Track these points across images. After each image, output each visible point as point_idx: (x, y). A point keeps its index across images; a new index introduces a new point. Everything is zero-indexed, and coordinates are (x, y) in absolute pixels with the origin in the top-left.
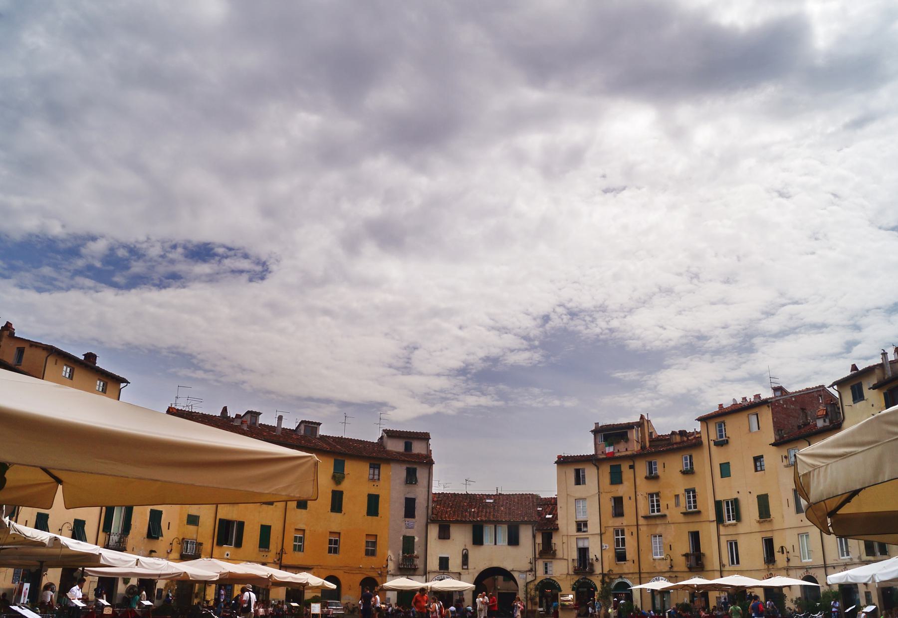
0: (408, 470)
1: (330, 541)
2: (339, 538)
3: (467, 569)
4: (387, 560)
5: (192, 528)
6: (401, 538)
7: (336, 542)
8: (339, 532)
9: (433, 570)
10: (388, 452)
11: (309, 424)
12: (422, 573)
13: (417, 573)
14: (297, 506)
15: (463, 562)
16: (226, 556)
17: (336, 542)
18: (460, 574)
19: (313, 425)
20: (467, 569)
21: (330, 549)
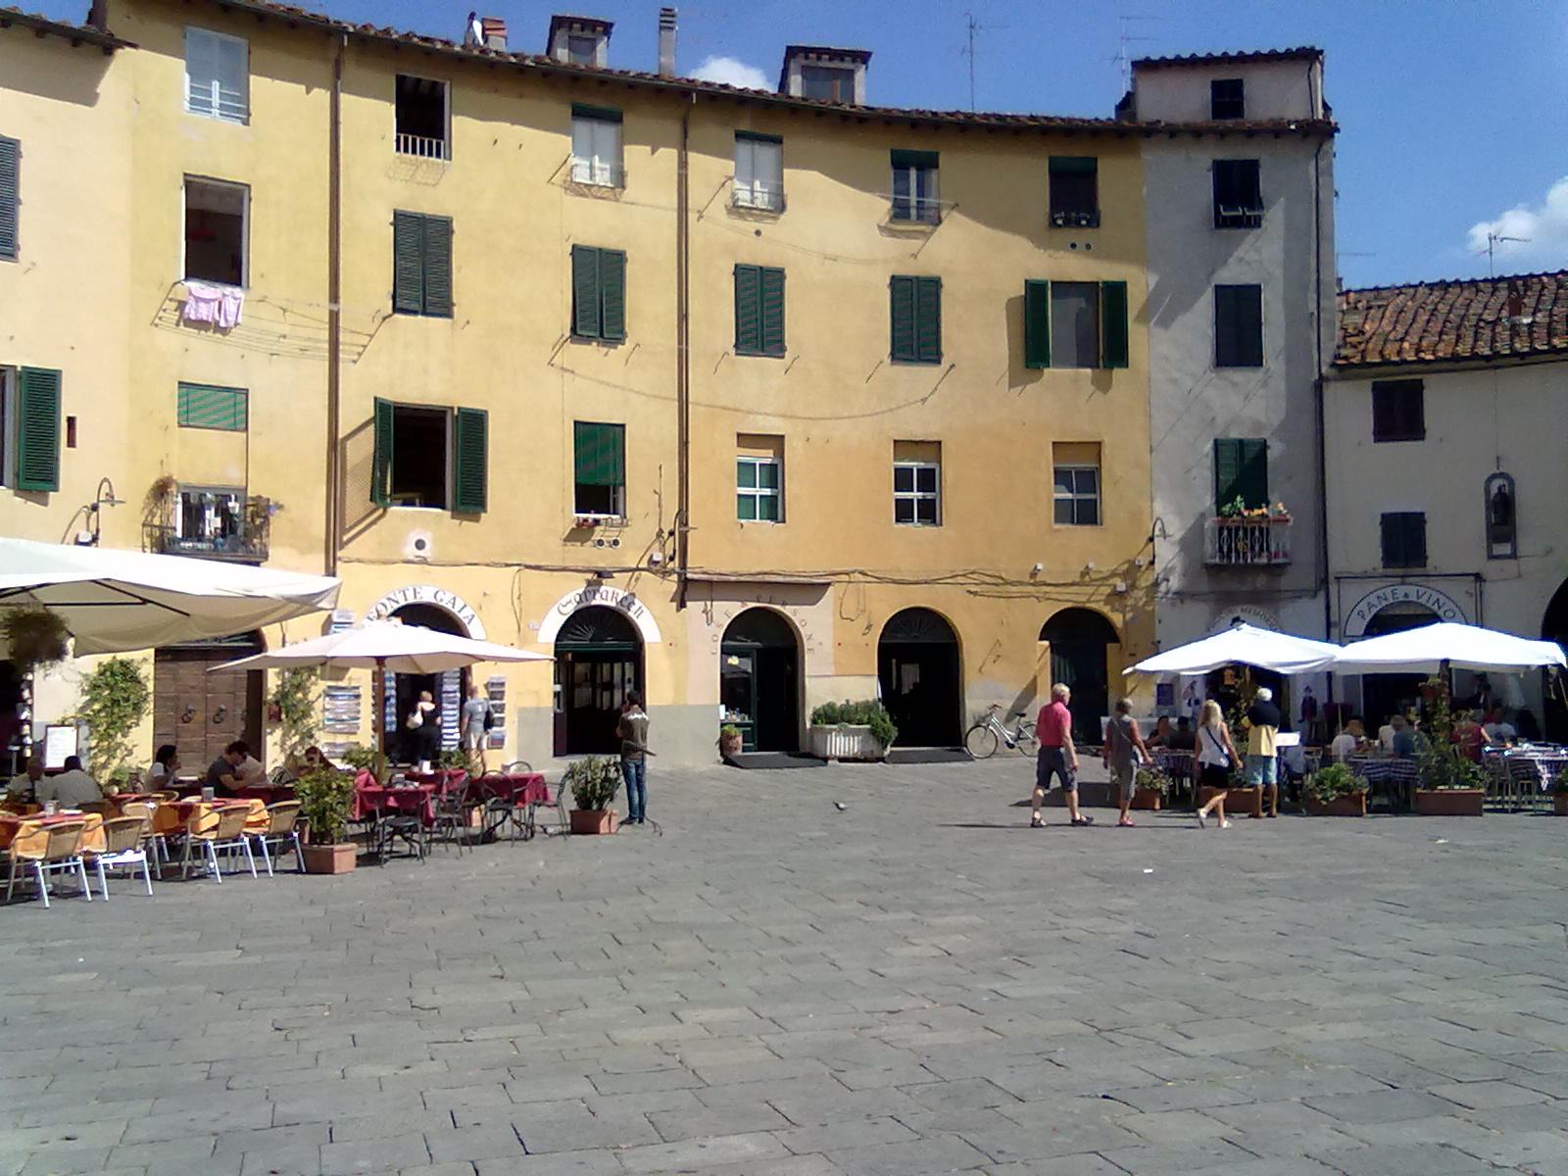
0: (1221, 170)
1: (902, 480)
2: (940, 462)
3: (1514, 556)
4: (1151, 539)
8: (936, 439)
9: (1358, 570)
12: (1310, 582)
13: (1286, 582)
14: (736, 346)
15: (1490, 527)
16: (411, 551)
17: (928, 480)
18: (1478, 577)
20: (1514, 556)
21: (903, 512)
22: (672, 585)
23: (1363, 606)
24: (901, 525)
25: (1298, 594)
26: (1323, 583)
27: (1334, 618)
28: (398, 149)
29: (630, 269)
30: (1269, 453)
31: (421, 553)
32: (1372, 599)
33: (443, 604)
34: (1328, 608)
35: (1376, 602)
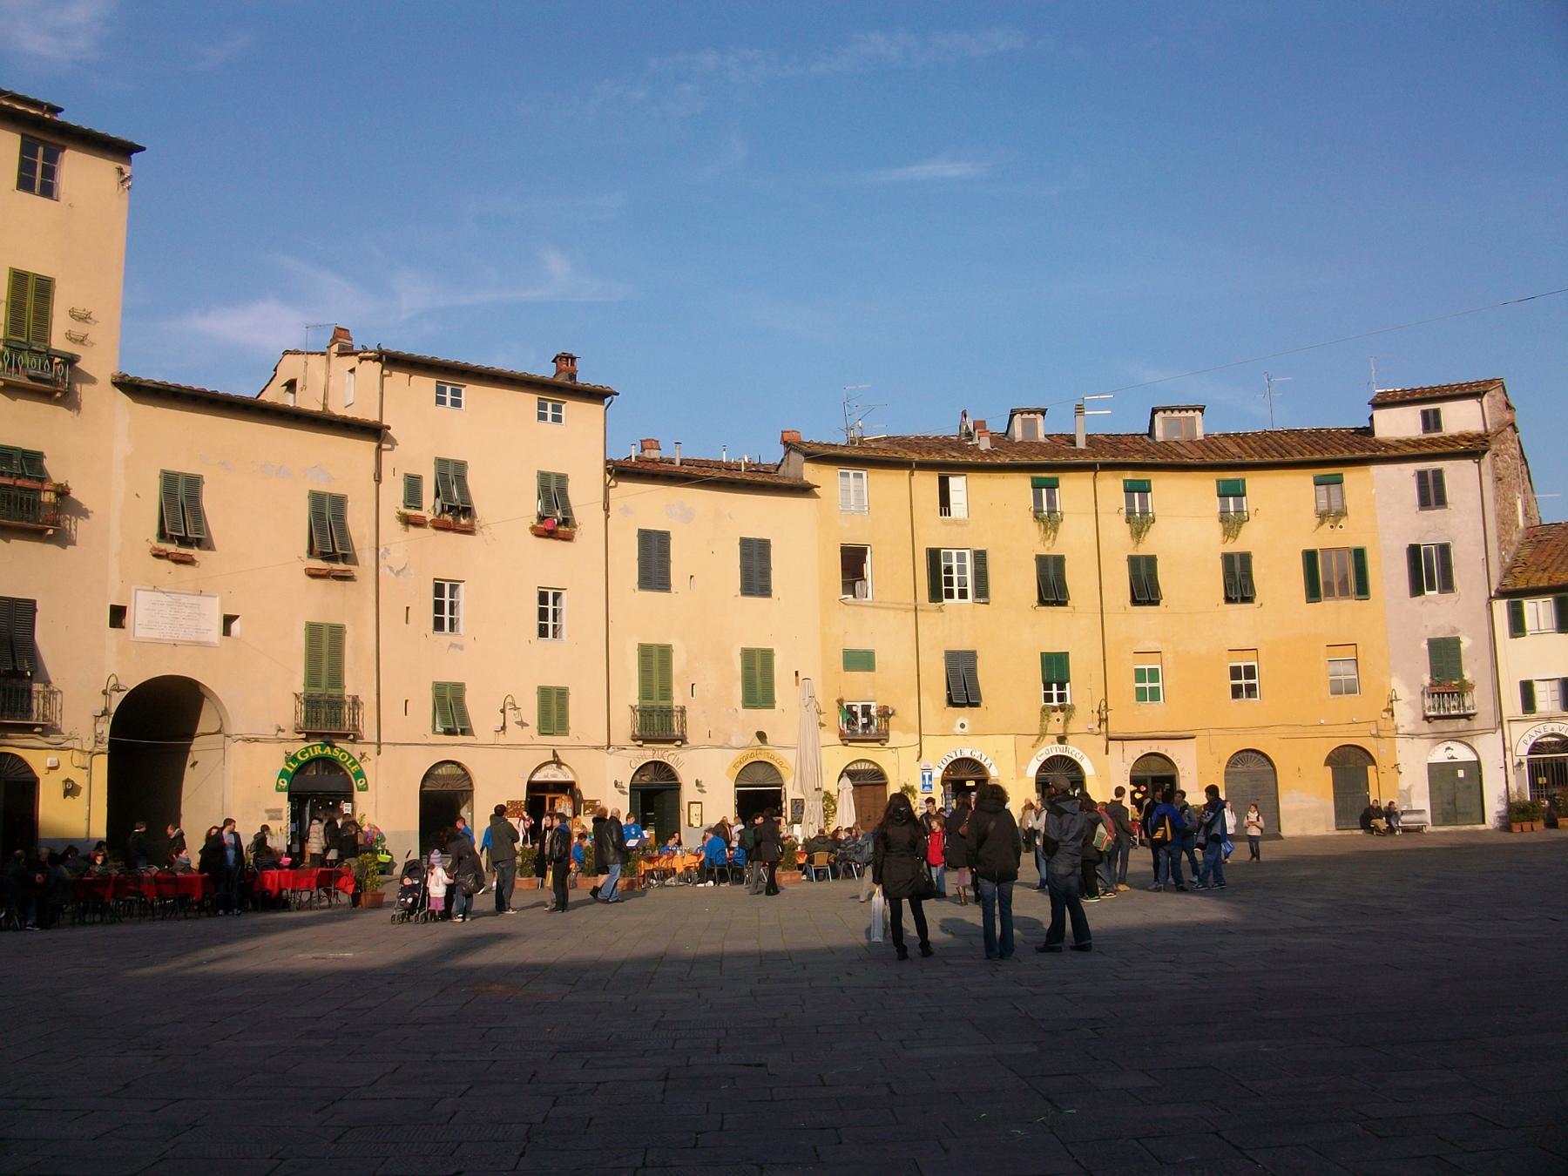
1: (1235, 673)
5: (859, 676)
6: (1424, 645)
7: (1250, 673)
10: (1385, 445)
11: (1172, 411)
12: (1491, 724)
13: (1476, 724)
16: (958, 729)
17: (1250, 673)
19: (1184, 414)
21: (1236, 691)
22: (1102, 740)
23: (1526, 737)
24: (1236, 700)
25: (1485, 731)
26: (1501, 722)
27: (1507, 745)
28: (941, 515)
29: (1067, 565)
30: (1462, 645)
31: (962, 730)
32: (1532, 732)
33: (975, 758)
34: (1504, 739)
35: (1534, 734)
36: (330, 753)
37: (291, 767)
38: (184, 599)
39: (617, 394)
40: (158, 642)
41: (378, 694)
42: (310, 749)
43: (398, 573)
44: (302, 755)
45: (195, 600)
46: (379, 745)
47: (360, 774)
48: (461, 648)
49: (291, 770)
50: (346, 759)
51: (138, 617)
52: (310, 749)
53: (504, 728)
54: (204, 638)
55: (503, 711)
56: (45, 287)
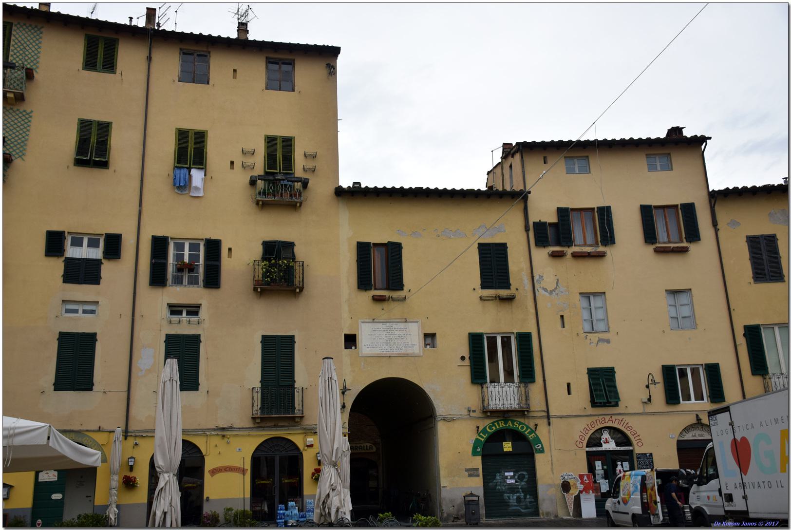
36: (511, 426)
37: (483, 438)
38: (394, 326)
39: (710, 138)
40: (379, 357)
41: (544, 380)
42: (496, 424)
43: (551, 292)
44: (490, 428)
45: (402, 325)
46: (548, 417)
47: (539, 441)
48: (608, 341)
49: (483, 440)
50: (524, 429)
51: (363, 340)
52: (496, 424)
53: (649, 400)
54: (410, 351)
55: (648, 387)
56: (288, 143)
